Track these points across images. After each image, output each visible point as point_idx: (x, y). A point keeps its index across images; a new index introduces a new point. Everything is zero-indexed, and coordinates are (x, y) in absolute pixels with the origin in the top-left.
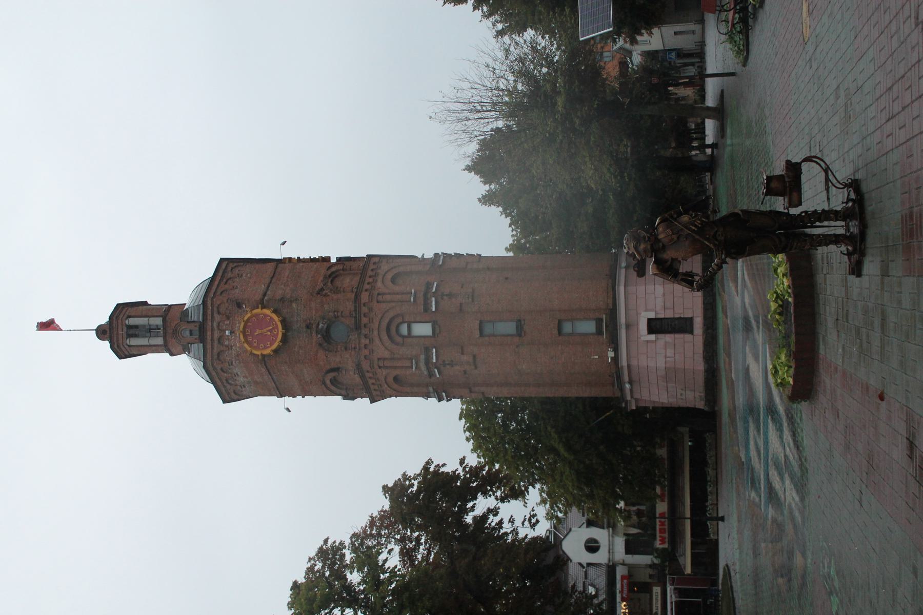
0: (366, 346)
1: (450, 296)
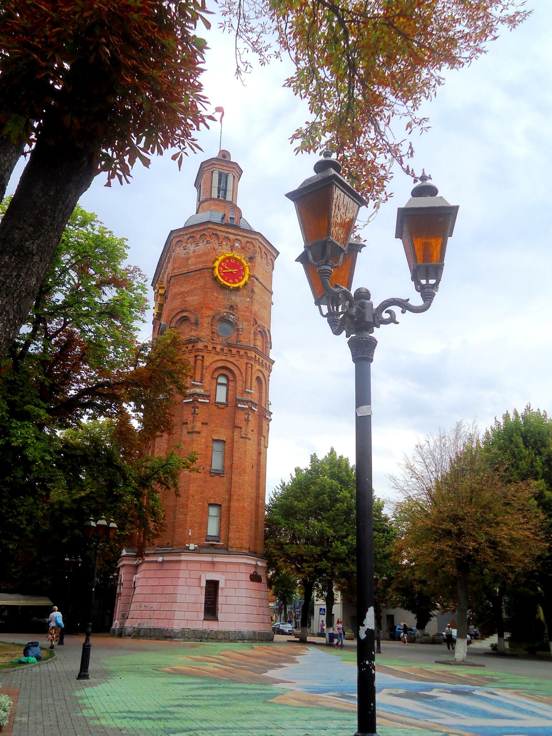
0: (214, 348)
1: (247, 420)
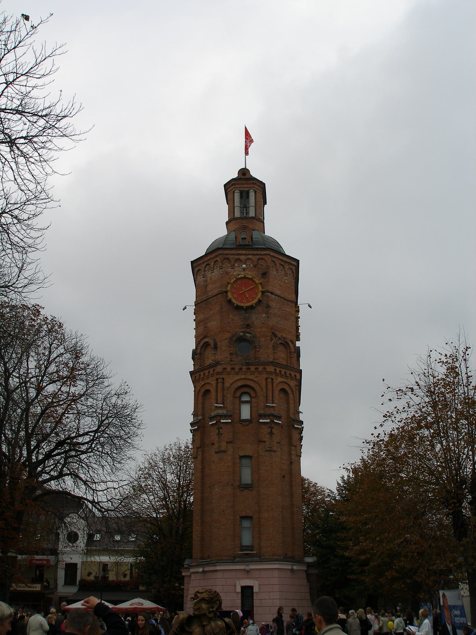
1: (271, 433)
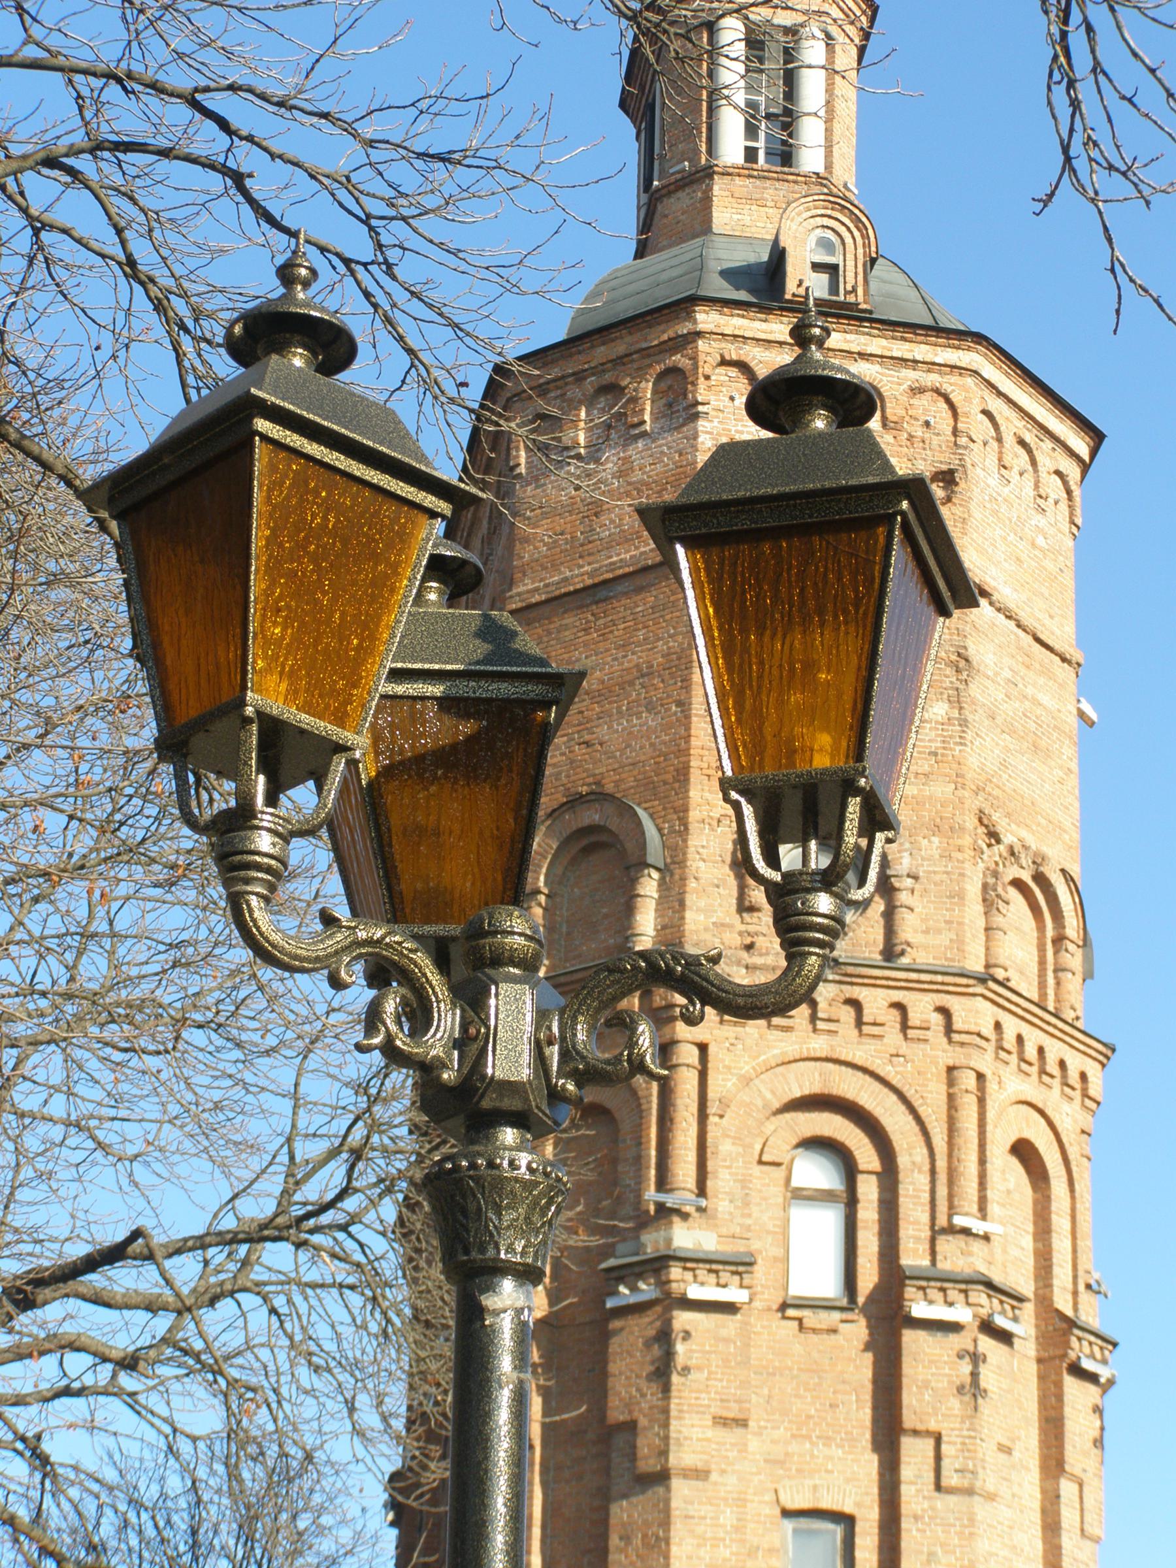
1: (973, 1389)
